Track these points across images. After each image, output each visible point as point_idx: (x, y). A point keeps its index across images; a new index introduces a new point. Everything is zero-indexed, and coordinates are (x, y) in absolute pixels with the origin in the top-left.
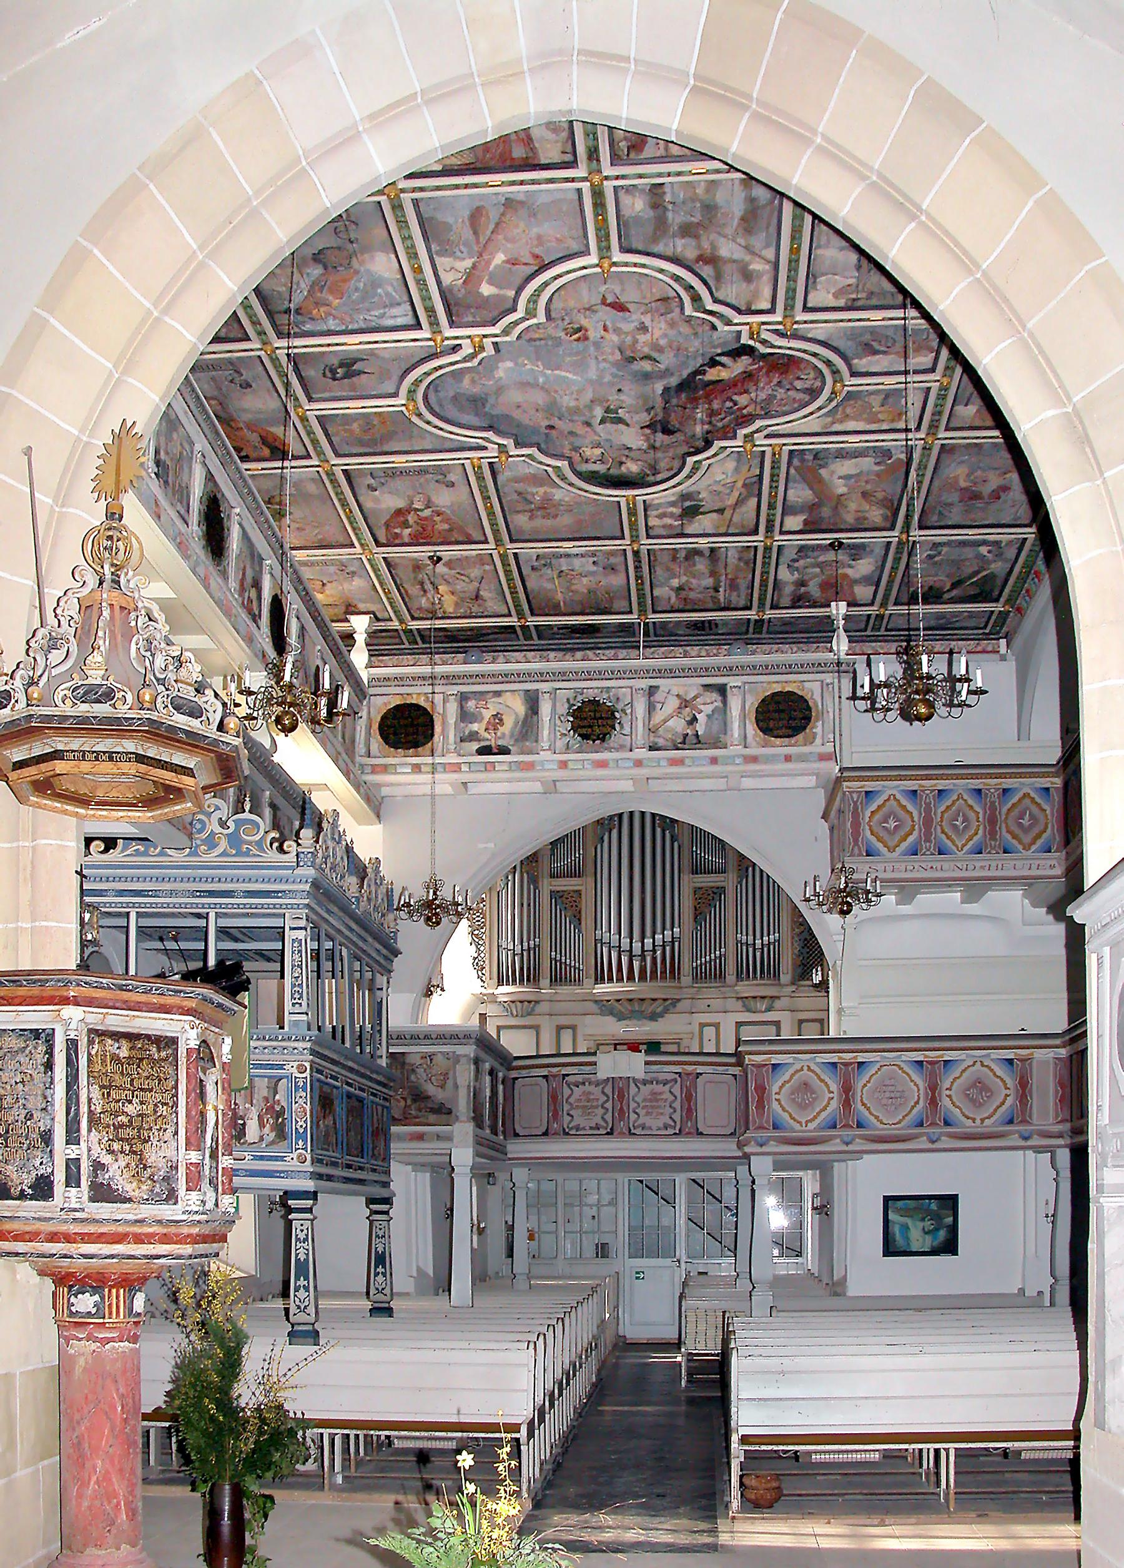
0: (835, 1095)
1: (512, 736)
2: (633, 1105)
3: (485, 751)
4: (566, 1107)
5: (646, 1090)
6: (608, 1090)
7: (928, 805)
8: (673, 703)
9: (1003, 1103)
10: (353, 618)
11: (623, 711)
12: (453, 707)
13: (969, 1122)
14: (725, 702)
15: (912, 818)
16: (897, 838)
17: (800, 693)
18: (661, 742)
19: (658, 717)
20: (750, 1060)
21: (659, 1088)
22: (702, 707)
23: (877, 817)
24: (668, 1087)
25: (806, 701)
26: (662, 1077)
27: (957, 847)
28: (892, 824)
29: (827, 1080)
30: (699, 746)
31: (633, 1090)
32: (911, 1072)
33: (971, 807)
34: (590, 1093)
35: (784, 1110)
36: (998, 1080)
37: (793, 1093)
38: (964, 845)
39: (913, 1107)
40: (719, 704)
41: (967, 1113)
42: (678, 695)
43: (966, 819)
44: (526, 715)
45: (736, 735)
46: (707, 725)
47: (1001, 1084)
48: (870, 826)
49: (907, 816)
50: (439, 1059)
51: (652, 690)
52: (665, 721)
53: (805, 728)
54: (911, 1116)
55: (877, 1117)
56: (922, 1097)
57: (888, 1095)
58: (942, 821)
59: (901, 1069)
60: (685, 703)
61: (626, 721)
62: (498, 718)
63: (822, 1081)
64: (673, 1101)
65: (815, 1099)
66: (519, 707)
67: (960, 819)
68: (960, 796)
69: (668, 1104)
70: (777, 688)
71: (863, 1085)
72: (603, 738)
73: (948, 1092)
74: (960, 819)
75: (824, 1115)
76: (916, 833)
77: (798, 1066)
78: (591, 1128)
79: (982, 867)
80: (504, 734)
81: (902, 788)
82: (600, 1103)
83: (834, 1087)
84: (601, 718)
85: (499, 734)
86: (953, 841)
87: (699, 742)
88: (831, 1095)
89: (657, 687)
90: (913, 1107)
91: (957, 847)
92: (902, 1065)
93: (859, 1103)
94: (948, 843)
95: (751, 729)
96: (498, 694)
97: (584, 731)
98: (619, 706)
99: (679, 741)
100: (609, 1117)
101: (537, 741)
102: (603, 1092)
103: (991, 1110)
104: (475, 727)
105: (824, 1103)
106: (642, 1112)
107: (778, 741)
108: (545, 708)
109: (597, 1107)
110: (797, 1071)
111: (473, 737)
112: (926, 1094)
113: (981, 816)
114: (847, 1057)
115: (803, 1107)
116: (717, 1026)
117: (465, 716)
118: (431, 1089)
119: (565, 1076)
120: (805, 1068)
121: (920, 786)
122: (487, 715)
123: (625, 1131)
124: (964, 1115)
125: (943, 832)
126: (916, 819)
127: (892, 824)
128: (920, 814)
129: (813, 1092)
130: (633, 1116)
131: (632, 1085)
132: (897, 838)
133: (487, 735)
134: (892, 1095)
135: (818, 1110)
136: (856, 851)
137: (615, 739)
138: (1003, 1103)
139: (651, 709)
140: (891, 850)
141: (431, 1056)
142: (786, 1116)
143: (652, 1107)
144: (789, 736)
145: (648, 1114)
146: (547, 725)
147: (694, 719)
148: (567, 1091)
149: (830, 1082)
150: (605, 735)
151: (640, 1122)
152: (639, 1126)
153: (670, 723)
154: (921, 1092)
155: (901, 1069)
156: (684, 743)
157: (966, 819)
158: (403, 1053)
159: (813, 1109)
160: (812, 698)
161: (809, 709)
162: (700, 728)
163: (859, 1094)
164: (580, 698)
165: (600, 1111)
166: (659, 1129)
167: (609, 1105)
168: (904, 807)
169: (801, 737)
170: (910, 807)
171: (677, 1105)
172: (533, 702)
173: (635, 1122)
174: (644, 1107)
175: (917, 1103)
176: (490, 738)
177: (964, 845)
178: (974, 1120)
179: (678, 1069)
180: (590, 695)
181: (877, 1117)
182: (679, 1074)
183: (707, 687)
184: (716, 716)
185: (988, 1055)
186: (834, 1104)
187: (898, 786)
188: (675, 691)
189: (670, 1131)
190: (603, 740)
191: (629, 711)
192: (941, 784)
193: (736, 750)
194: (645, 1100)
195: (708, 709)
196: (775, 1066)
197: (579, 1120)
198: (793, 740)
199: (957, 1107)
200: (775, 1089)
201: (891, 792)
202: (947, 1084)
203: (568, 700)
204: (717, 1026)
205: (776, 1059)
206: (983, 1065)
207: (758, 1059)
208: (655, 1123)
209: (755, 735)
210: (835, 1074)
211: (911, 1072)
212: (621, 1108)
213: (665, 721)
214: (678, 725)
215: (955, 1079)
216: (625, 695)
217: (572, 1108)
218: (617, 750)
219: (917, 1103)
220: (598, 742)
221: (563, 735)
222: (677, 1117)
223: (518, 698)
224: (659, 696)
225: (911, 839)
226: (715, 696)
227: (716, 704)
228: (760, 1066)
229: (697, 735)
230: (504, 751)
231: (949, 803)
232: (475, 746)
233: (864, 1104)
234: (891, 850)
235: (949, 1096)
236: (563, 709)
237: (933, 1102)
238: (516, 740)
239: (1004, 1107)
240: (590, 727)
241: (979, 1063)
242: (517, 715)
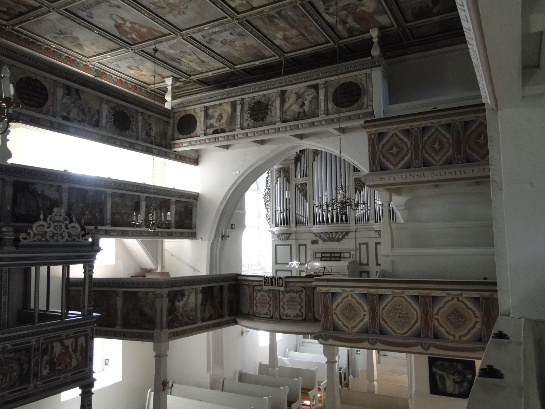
0: (367, 313)
1: (226, 124)
2: (282, 303)
3: (216, 132)
4: (255, 302)
5: (287, 295)
6: (271, 295)
7: (416, 137)
8: (293, 97)
9: (474, 327)
10: (166, 80)
11: (272, 105)
12: (202, 114)
13: (451, 338)
14: (318, 93)
15: (407, 146)
16: (398, 159)
17: (355, 82)
18: (288, 117)
19: (287, 105)
20: (320, 290)
21: (294, 295)
22: (307, 97)
23: (386, 148)
24: (298, 294)
25: (358, 86)
26: (295, 289)
27: (435, 160)
28: (395, 151)
29: (362, 303)
30: (306, 117)
31: (282, 295)
32: (412, 302)
33: (444, 135)
34: (263, 296)
35: (339, 319)
36: (470, 311)
37: (343, 310)
38: (440, 160)
39: (414, 324)
40: (315, 94)
41: (449, 331)
42: (296, 93)
43: (441, 143)
44: (232, 113)
45: (323, 108)
46: (309, 106)
47: (471, 313)
48: (382, 153)
49: (404, 145)
50: (150, 295)
51: (283, 93)
52: (290, 107)
53: (358, 100)
54: (413, 330)
55: (392, 329)
56: (419, 317)
57: (398, 315)
58: (425, 146)
59: (405, 299)
60: (299, 96)
61: (273, 109)
62: (221, 116)
63: (359, 304)
64: (302, 302)
65: (356, 314)
66: (228, 109)
67: (437, 143)
68: (437, 130)
69: (298, 303)
70: (344, 81)
71: (385, 307)
72: (263, 119)
73: (436, 317)
74: (437, 143)
75: (361, 324)
76: (409, 155)
77: (345, 294)
78: (264, 314)
79: (451, 173)
80: (223, 123)
81: (399, 129)
82: (267, 301)
83: (366, 308)
84: (262, 110)
85: (221, 123)
86: (433, 158)
87: (306, 115)
88: (365, 313)
89: (286, 91)
90: (414, 324)
91: (435, 160)
92: (406, 297)
93: (381, 320)
94: (431, 159)
95: (331, 105)
96: (220, 105)
97: (255, 117)
98: (270, 103)
99: (296, 116)
100: (271, 309)
101: (236, 125)
102: (269, 296)
103: (466, 331)
104: (212, 121)
105: (361, 318)
106: (286, 307)
107: (344, 109)
108: (239, 108)
109: (266, 303)
110: (345, 297)
111: (211, 126)
112: (422, 317)
113: (450, 140)
114: (372, 291)
115: (350, 319)
116: (367, 244)
117: (207, 116)
118: (147, 310)
119: (255, 286)
120: (350, 296)
121: (411, 126)
122: (216, 115)
123: (278, 317)
124: (447, 332)
125: (426, 152)
126: (409, 146)
127: (395, 151)
128: (411, 143)
129: (354, 310)
130: (282, 310)
131: (281, 293)
132: (398, 159)
133: (216, 125)
134: (401, 316)
135: (357, 321)
136: (374, 168)
137: (268, 119)
138: (474, 327)
139: (283, 102)
140: (395, 165)
141: (147, 293)
142: (340, 323)
143: (291, 305)
144: (350, 106)
145: (289, 308)
146: (239, 117)
147: (303, 104)
148: (255, 294)
149: (364, 305)
150: (264, 118)
151: (286, 312)
152: (285, 315)
153: (292, 108)
154: (419, 315)
155: (405, 299)
156: (298, 116)
157: (441, 143)
158: (136, 292)
159: (355, 321)
160: (361, 83)
161: (360, 89)
162: (306, 108)
163: (381, 314)
164: (253, 101)
165: (268, 306)
166: (294, 317)
167: (271, 303)
168: (402, 140)
169: (355, 106)
170: (405, 139)
171: (303, 304)
172: (234, 105)
173: (283, 312)
174: (287, 305)
175: (416, 321)
176: (218, 126)
177: (440, 160)
178: (454, 336)
179: (303, 285)
180: (257, 99)
181: (392, 329)
182: (304, 287)
183: (309, 87)
184: (313, 100)
185: (462, 294)
186: (366, 319)
187: (397, 128)
188: (294, 92)
189: (300, 318)
190: (263, 120)
191: (274, 105)
192: (424, 123)
193: (323, 117)
194: (287, 301)
195: (309, 98)
196: (333, 294)
197: (260, 310)
198: (352, 108)
199: (443, 327)
200: (334, 306)
201: (393, 132)
202: (435, 311)
203: (248, 103)
204: (367, 244)
205: (333, 290)
206: (458, 300)
207: (324, 289)
208: (292, 313)
209: (333, 108)
210: (366, 300)
211: (412, 302)
212: (276, 304)
213: (290, 107)
214: (296, 108)
215: (440, 309)
216: (272, 96)
217: (257, 303)
218: (269, 125)
219: (416, 321)
220: (261, 122)
221: (247, 120)
222: (303, 310)
223: (228, 105)
224: (287, 95)
225: (407, 158)
226: (313, 90)
227: (314, 95)
228: (325, 293)
229: (304, 112)
230: (223, 131)
231: (430, 134)
232: (211, 130)
233: (384, 320)
234: (395, 165)
235: (437, 319)
236: (246, 108)
237: (426, 322)
238: (228, 125)
239: (474, 331)
240: (257, 114)
241: (455, 299)
242: (228, 114)
